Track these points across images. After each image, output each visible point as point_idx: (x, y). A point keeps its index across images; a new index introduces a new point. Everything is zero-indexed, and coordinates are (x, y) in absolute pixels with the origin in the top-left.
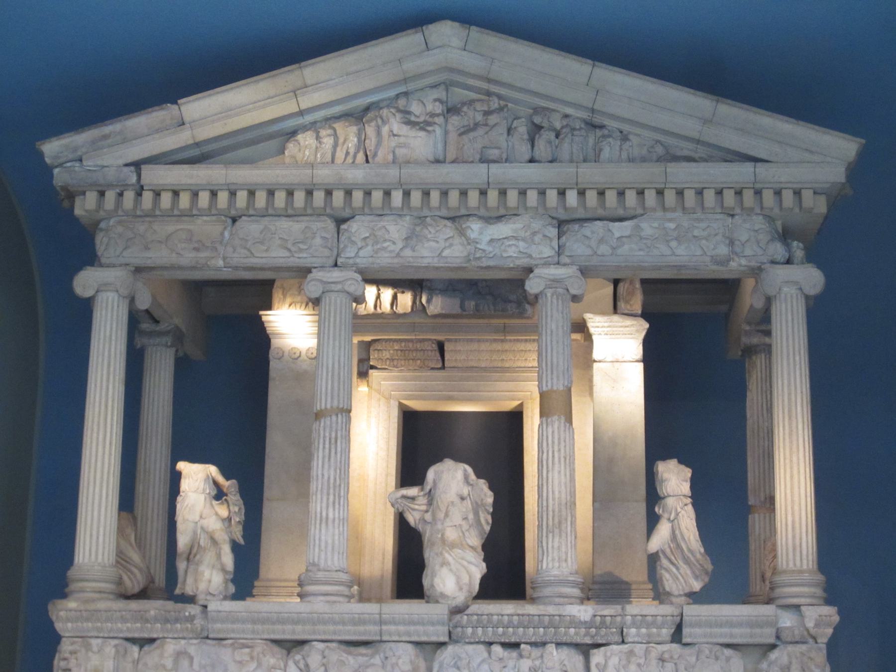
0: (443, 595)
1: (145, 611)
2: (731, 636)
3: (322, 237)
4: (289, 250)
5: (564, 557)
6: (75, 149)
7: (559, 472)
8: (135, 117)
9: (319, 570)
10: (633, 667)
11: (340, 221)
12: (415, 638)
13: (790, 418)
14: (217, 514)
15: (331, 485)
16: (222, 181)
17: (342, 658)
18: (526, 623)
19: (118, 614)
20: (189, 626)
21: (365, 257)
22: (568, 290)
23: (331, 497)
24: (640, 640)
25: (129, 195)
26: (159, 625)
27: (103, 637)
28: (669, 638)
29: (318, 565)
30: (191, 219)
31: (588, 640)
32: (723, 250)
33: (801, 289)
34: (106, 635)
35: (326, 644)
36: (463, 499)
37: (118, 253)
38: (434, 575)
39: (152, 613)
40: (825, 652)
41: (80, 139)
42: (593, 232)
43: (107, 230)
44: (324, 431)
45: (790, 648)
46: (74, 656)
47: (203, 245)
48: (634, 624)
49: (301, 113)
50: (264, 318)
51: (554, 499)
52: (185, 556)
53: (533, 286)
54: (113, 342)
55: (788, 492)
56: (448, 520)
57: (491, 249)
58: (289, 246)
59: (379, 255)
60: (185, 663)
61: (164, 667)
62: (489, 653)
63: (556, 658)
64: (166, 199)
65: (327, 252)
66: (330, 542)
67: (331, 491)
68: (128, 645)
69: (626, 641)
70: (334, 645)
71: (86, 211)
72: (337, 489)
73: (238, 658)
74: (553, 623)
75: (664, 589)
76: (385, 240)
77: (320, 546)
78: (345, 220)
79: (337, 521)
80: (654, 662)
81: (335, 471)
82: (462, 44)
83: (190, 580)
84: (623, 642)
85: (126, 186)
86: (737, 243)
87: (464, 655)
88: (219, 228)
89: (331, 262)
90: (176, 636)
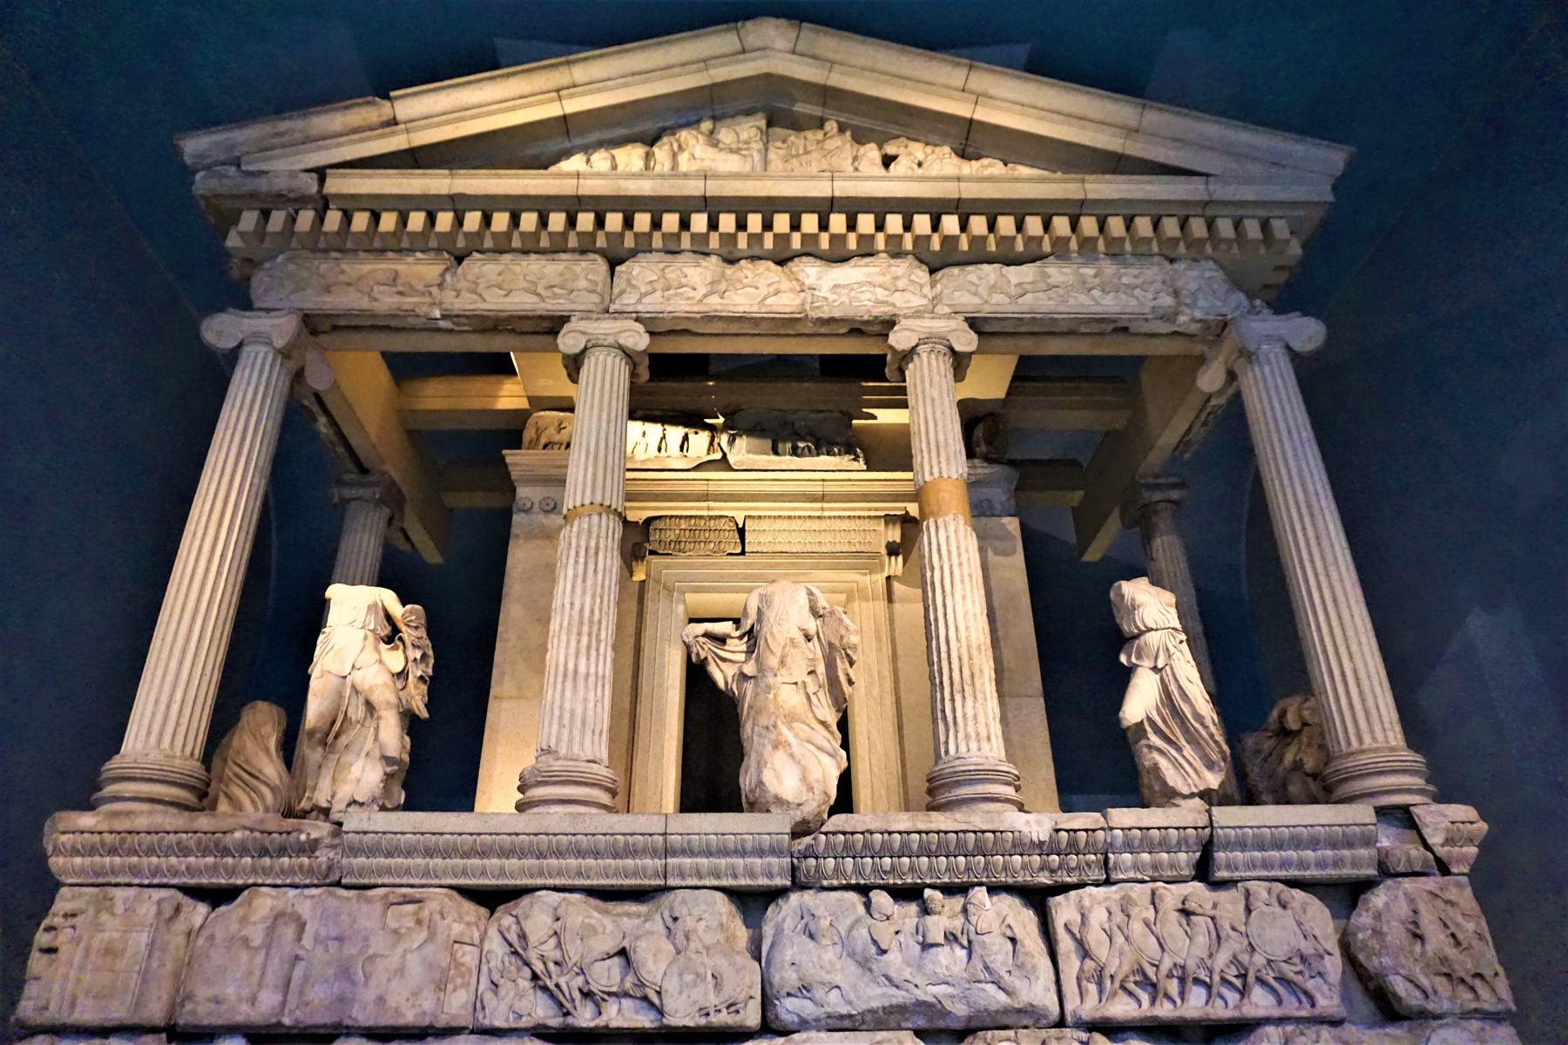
0: (779, 801)
2: (1302, 865)
4: (539, 295)
5: (984, 734)
6: (231, 148)
7: (964, 597)
8: (326, 112)
10: (1137, 927)
11: (614, 263)
12: (727, 882)
13: (1312, 516)
14: (381, 662)
15: (586, 620)
16: (444, 191)
17: (593, 922)
18: (934, 848)
19: (172, 838)
21: (652, 304)
22: (952, 349)
23: (585, 640)
24: (1140, 876)
25: (306, 218)
27: (140, 885)
28: (1187, 872)
31: (1044, 879)
32: (1167, 301)
33: (1288, 348)
34: (146, 882)
35: (562, 895)
36: (808, 639)
38: (760, 765)
39: (238, 835)
40: (1468, 891)
41: (244, 136)
42: (980, 279)
45: (1407, 883)
46: (71, 921)
47: (411, 287)
48: (1128, 846)
49: (564, 123)
50: (508, 460)
51: (958, 639)
53: (900, 339)
55: (1335, 623)
56: (783, 671)
57: (832, 297)
58: (540, 290)
60: (289, 932)
61: (246, 941)
62: (868, 905)
63: (991, 915)
64: (361, 221)
65: (595, 298)
66: (579, 711)
67: (585, 629)
68: (187, 901)
69: (1115, 876)
70: (577, 896)
71: (242, 234)
73: (392, 924)
74: (984, 845)
75: (1165, 783)
77: (561, 717)
78: (621, 262)
79: (592, 679)
80: (1174, 916)
81: (593, 597)
82: (791, 45)
83: (325, 784)
84: (1108, 882)
85: (301, 201)
86: (1184, 292)
87: (820, 912)
88: (437, 269)
89: (601, 307)
90: (279, 882)
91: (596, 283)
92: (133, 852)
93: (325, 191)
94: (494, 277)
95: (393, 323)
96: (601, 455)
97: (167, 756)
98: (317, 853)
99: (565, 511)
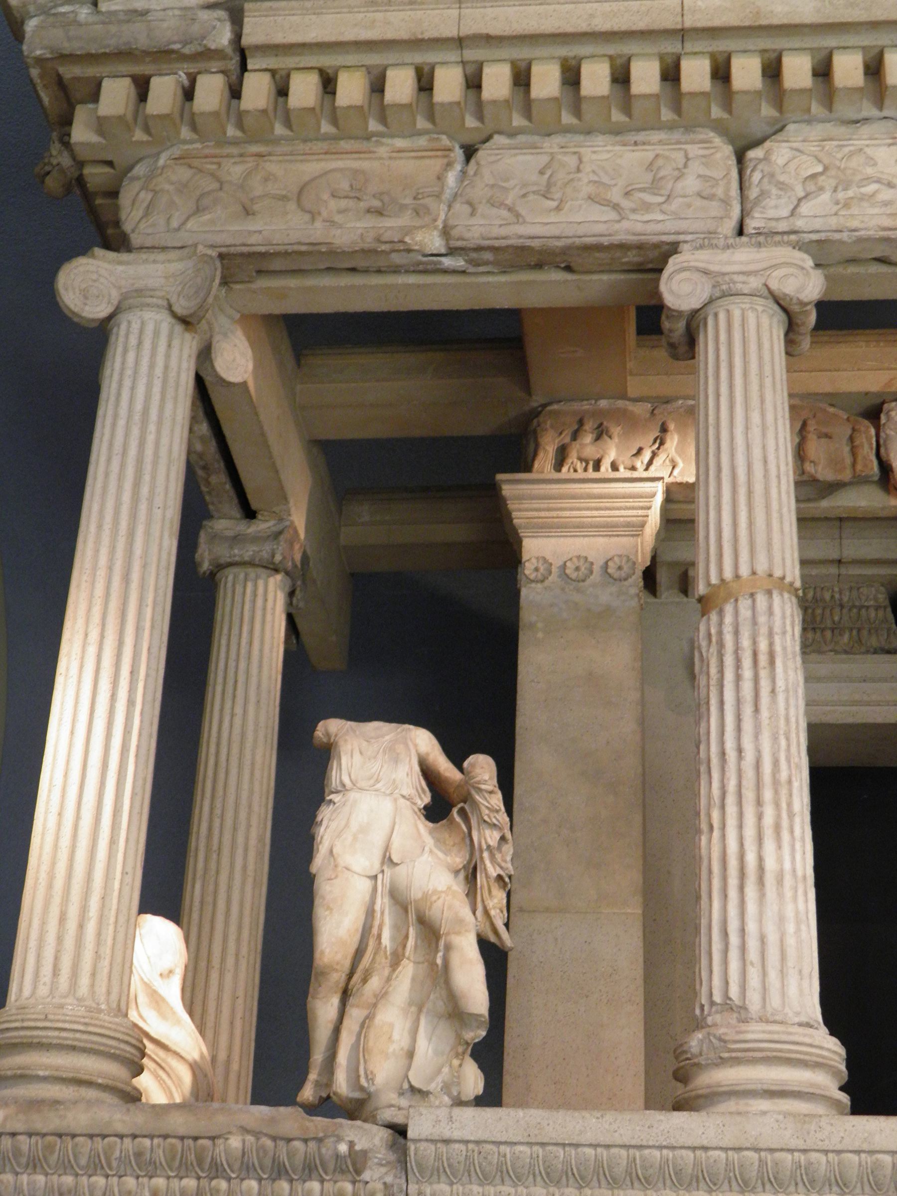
1: (213, 1138)
3: (699, 176)
4: (616, 207)
9: (745, 1021)
20: (349, 1187)
21: (818, 214)
25: (210, 90)
26: (254, 1184)
29: (744, 1008)
30: (364, 146)
37: (175, 224)
39: (235, 1142)
43: (150, 177)
44: (736, 633)
50: (507, 490)
52: (337, 977)
54: (152, 428)
58: (615, 195)
59: (855, 210)
66: (772, 938)
67: (768, 795)
72: (784, 792)
76: (869, 180)
77: (743, 948)
78: (757, 143)
79: (788, 881)
81: (775, 738)
85: (207, 54)
89: (731, 224)
91: (714, 182)
92: (66, 1167)
93: (246, 41)
94: (534, 177)
95: (361, 263)
96: (758, 488)
97: (89, 1010)
98: (366, 1175)
99: (701, 589)
